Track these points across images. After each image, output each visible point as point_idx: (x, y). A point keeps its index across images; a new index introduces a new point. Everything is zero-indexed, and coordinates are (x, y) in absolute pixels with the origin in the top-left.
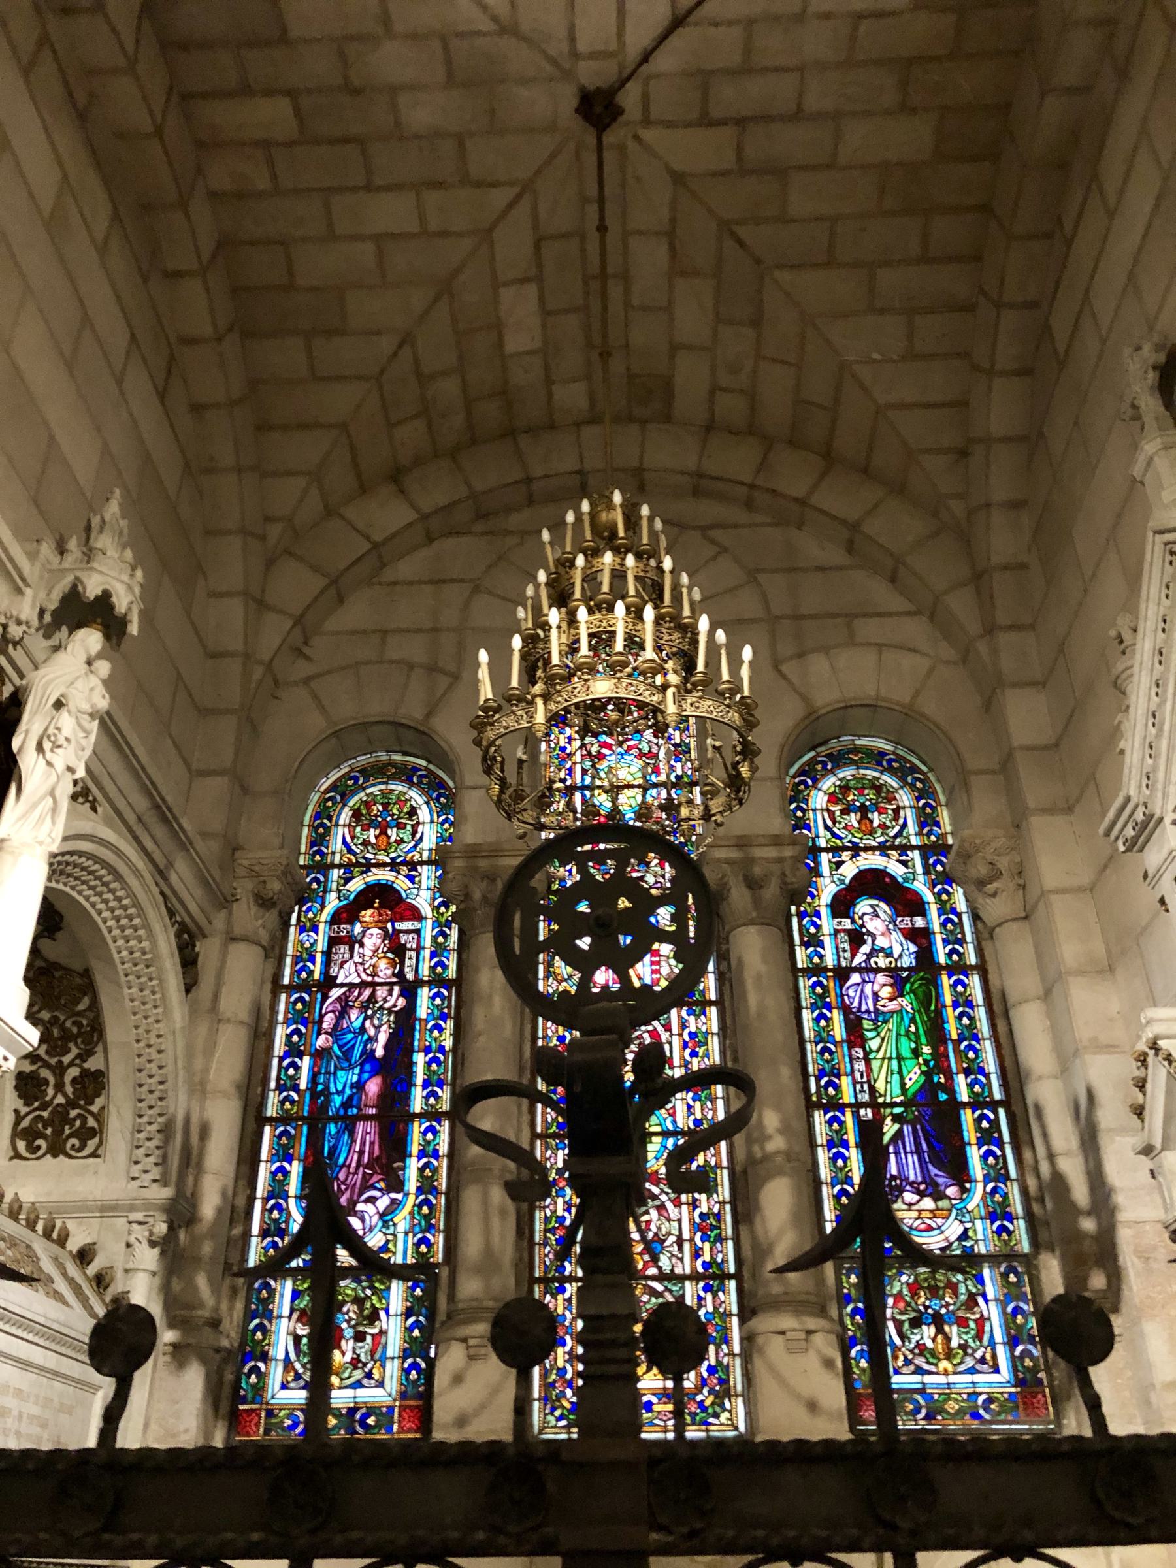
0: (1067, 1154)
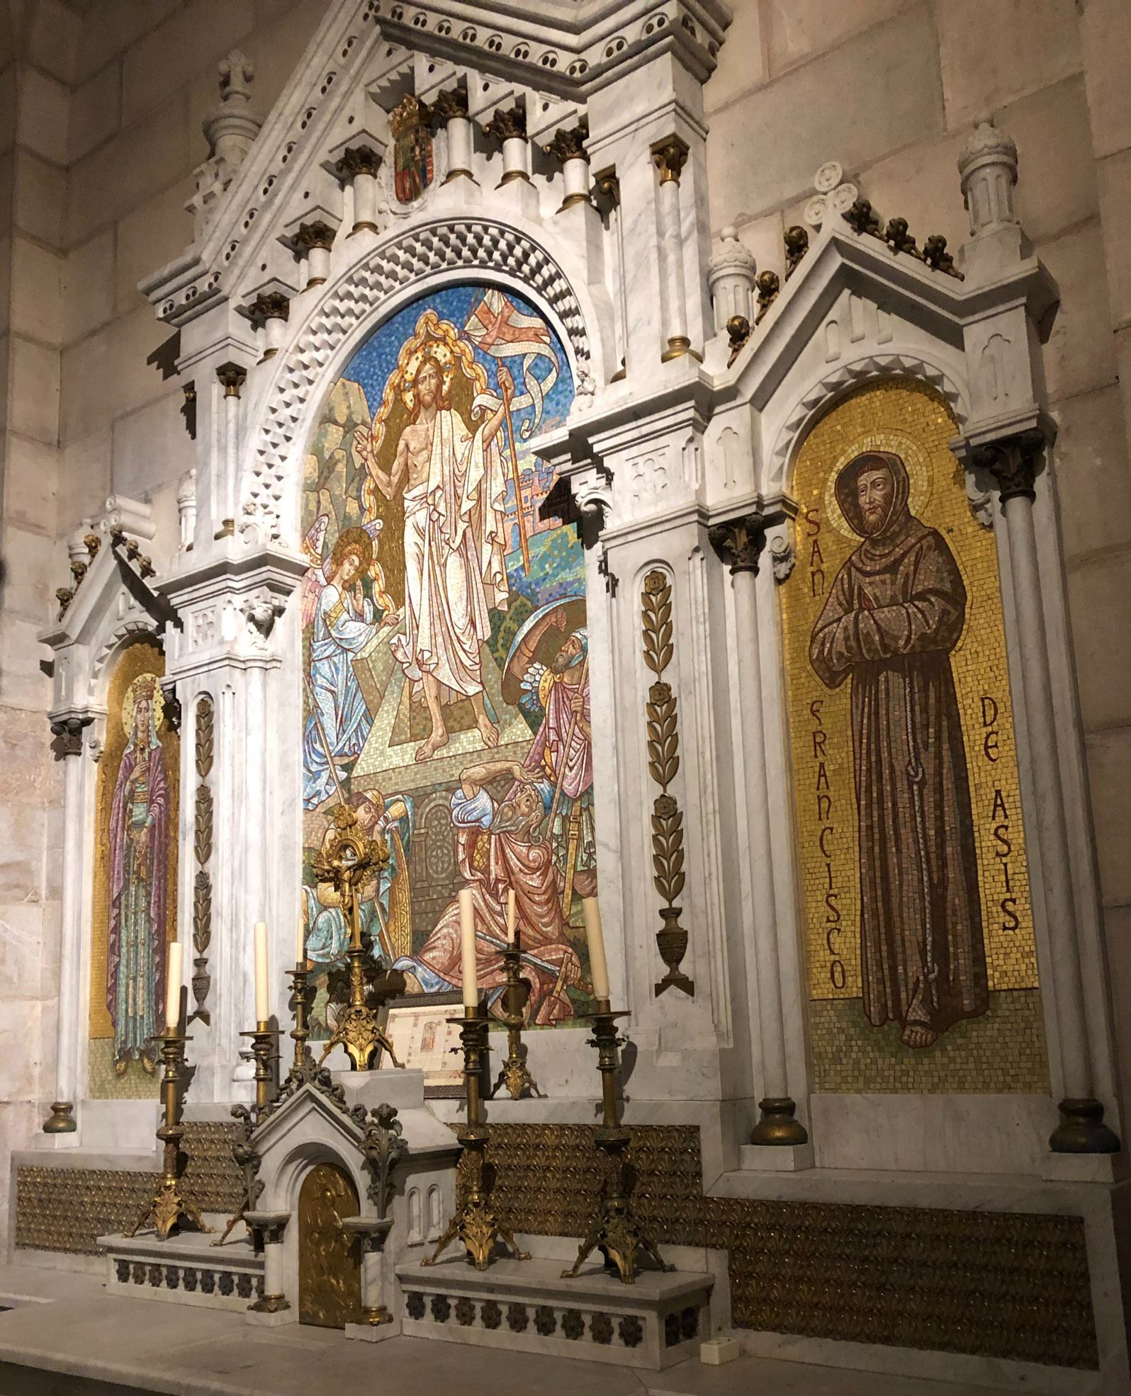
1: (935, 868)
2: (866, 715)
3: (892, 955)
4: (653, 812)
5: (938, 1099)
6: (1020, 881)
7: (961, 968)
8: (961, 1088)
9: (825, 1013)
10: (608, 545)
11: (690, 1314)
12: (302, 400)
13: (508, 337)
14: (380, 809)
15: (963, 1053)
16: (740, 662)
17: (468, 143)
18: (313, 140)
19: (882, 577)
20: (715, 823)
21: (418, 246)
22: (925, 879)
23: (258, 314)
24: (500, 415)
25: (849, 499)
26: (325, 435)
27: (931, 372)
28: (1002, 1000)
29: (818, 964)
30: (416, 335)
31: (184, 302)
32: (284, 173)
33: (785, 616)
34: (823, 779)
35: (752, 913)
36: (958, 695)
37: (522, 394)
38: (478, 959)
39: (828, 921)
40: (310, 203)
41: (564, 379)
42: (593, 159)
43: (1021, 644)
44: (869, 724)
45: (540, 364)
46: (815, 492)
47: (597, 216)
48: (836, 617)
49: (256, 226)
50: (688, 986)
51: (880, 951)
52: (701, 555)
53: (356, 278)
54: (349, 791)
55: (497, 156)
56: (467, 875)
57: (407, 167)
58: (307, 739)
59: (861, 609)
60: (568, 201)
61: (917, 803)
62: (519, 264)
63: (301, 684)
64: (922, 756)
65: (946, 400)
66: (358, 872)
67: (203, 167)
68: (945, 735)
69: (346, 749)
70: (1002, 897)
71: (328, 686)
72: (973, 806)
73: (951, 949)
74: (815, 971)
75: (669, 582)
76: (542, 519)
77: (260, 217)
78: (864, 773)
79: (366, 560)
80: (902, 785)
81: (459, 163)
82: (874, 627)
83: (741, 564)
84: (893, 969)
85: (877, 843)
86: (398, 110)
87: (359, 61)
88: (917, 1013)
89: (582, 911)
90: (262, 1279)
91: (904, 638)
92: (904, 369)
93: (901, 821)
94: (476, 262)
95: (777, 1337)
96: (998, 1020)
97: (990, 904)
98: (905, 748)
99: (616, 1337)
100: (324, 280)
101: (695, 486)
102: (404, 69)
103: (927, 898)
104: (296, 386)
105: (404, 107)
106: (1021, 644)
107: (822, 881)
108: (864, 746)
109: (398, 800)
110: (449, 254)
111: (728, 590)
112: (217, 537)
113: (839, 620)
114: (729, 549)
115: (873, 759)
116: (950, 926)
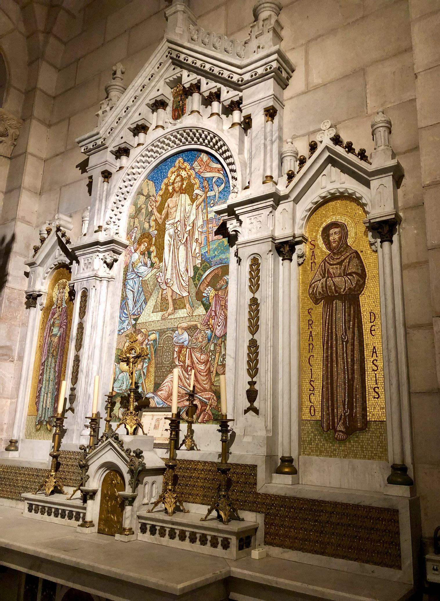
1: (350, 374)
2: (328, 315)
3: (333, 405)
5: (346, 461)
6: (381, 381)
7: (358, 411)
8: (355, 457)
9: (307, 425)
10: (239, 247)
12: (131, 186)
14: (146, 336)
15: (357, 444)
16: (283, 292)
17: (199, 102)
18: (144, 96)
19: (336, 266)
20: (270, 350)
21: (178, 135)
22: (346, 377)
24: (203, 197)
25: (326, 238)
26: (139, 199)
27: (358, 195)
28: (372, 425)
29: (305, 406)
30: (175, 167)
31: (92, 147)
32: (133, 106)
33: (300, 277)
34: (311, 338)
35: (282, 385)
36: (362, 311)
37: (212, 190)
39: (310, 390)
40: (140, 117)
41: (227, 187)
42: (243, 111)
43: (385, 295)
44: (329, 318)
45: (219, 181)
46: (314, 234)
47: (243, 131)
48: (319, 279)
53: (155, 144)
54: (135, 328)
55: (209, 107)
56: (177, 363)
57: (176, 108)
58: (122, 308)
59: (328, 277)
60: (233, 125)
61: (345, 349)
62: (214, 145)
63: (122, 288)
64: (347, 332)
65: (363, 205)
66: (136, 359)
67: (103, 101)
68: (356, 325)
69: (136, 313)
70: (374, 386)
71: (131, 289)
72: (365, 352)
73: (354, 404)
74: (304, 409)
75: (260, 261)
76: (215, 235)
77: (122, 121)
78: (326, 336)
79: (150, 244)
80: (340, 342)
81: (195, 108)
82: (332, 284)
84: (333, 410)
85: (329, 362)
86: (175, 88)
87: (163, 71)
88: (340, 427)
89: (219, 380)
90: (85, 514)
91: (343, 289)
92: (348, 194)
94: (199, 143)
96: (370, 432)
97: (369, 388)
98: (341, 328)
100: (143, 144)
101: (271, 228)
102: (179, 75)
103: (347, 384)
104: (130, 180)
105: (178, 88)
106: (385, 295)
107: (309, 375)
108: (327, 326)
109: (154, 333)
111: (281, 267)
112: (95, 232)
113: (320, 280)
114: (282, 252)
115: (330, 331)
116: (354, 395)
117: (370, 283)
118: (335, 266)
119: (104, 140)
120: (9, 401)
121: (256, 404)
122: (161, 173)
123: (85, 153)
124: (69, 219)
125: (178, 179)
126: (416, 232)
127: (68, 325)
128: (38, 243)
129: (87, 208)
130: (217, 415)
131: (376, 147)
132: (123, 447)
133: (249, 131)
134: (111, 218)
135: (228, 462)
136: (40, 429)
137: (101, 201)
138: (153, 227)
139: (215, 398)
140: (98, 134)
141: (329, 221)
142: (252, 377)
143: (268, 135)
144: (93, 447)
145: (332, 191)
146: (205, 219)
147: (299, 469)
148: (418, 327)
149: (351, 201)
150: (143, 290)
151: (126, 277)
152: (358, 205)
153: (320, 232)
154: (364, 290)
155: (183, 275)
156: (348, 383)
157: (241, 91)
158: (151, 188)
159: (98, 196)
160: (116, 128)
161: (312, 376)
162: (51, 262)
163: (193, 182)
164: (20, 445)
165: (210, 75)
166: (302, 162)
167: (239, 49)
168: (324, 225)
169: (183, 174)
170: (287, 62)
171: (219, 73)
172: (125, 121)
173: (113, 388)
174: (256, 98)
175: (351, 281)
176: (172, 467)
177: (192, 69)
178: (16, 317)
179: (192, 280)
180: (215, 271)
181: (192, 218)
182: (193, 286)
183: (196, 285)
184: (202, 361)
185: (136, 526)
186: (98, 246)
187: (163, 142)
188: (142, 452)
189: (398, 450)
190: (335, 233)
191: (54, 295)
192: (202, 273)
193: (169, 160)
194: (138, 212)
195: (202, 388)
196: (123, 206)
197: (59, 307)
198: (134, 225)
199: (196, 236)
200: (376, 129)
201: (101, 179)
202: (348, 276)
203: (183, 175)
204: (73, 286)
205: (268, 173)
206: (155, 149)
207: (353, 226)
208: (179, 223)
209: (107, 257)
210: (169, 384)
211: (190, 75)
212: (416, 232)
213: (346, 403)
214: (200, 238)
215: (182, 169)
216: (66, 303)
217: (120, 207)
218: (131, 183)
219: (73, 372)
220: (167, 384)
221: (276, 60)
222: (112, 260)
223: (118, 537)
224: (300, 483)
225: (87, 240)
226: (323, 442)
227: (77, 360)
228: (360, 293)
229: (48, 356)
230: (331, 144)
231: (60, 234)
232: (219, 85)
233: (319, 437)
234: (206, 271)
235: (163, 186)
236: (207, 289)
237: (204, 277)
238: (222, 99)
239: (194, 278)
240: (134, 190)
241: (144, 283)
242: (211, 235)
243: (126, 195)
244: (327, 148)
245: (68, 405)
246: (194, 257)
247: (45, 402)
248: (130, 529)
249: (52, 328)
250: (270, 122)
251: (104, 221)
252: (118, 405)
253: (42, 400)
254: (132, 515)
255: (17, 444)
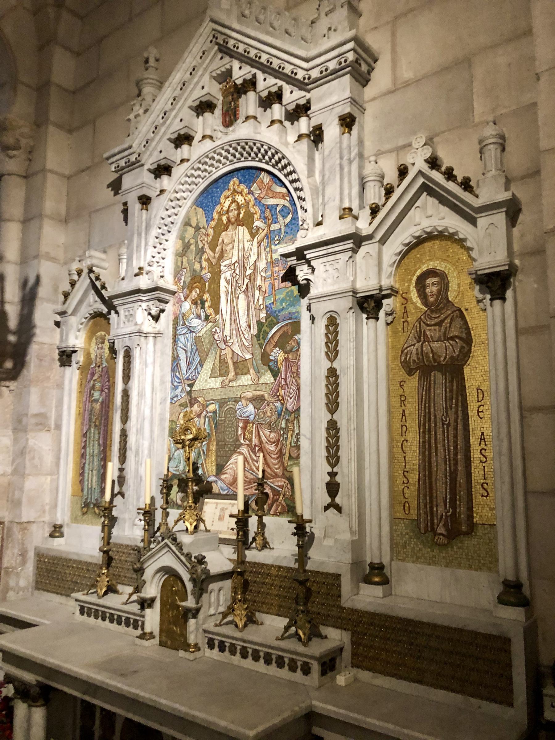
0: (11, 303)
1: (452, 465)
2: (424, 390)
4: (326, 426)
5: (448, 572)
8: (459, 566)
10: (311, 301)
11: (333, 660)
13: (271, 196)
14: (204, 407)
15: (461, 551)
16: (368, 360)
17: (256, 104)
18: (186, 95)
19: (435, 327)
20: (354, 434)
22: (448, 469)
23: (157, 172)
25: (422, 290)
28: (479, 528)
32: (172, 110)
33: (390, 340)
34: (404, 418)
36: (467, 386)
37: (276, 223)
38: (245, 480)
41: (295, 218)
44: (426, 394)
45: (284, 209)
46: (406, 284)
48: (413, 343)
49: (158, 133)
50: (339, 509)
51: (427, 508)
52: (353, 311)
53: (202, 161)
54: (191, 396)
55: (268, 110)
56: (242, 441)
57: (227, 111)
58: (173, 370)
59: (424, 341)
60: (300, 137)
61: (446, 434)
63: (171, 345)
64: (449, 412)
66: (193, 442)
68: (460, 404)
69: (190, 377)
70: (482, 481)
71: (183, 347)
72: (471, 438)
73: (458, 503)
75: (338, 321)
76: (282, 282)
77: (160, 130)
78: (422, 417)
80: (439, 424)
81: (251, 113)
82: (430, 350)
83: (371, 316)
84: (431, 508)
85: (427, 449)
86: (225, 84)
87: (208, 61)
88: (441, 530)
91: (444, 357)
93: (438, 441)
94: (257, 159)
95: (371, 674)
96: (477, 537)
97: (476, 484)
98: (442, 407)
99: (299, 670)
101: (352, 278)
102: (228, 66)
105: (227, 83)
108: (423, 404)
109: (213, 403)
110: (245, 154)
113: (414, 345)
114: (366, 308)
115: (427, 411)
116: (458, 492)
117: (477, 350)
118: (433, 328)
119: (139, 156)
120: (49, 478)
121: (338, 500)
122: (212, 197)
123: (116, 172)
124: (103, 256)
125: (234, 206)
126: (535, 286)
127: (111, 389)
128: (67, 287)
129: (123, 241)
130: (292, 507)
131: (485, 172)
132: (182, 550)
133: (320, 145)
134: (153, 257)
135: (307, 568)
136: (87, 512)
137: (139, 235)
138: (205, 268)
139: (289, 486)
140: (130, 147)
141: (424, 268)
142: (333, 466)
143: (345, 152)
144: (147, 549)
145: (428, 230)
146: (269, 261)
147: (391, 576)
148: (538, 409)
149: (452, 242)
150: (197, 349)
151: (176, 332)
152: (462, 248)
153: (414, 282)
154: (470, 360)
155: (244, 332)
156: (450, 476)
157: (308, 91)
158: (200, 217)
159: (136, 228)
160: (153, 139)
161: (405, 466)
162: (85, 311)
163: (252, 210)
164: (65, 530)
165: (267, 69)
166: (389, 191)
167: (304, 31)
168: (418, 273)
169: (240, 199)
170: (367, 50)
171: (280, 67)
172: (163, 129)
173: (168, 468)
174: (328, 102)
175: (453, 348)
176: (241, 574)
177: (245, 59)
178: (48, 378)
179: (255, 339)
180: (283, 328)
181: (253, 258)
182: (257, 346)
183: (261, 345)
184: (271, 440)
185: (203, 643)
186: (140, 294)
187: (213, 158)
188: (204, 557)
189: (510, 562)
190: (433, 284)
191: (92, 351)
192: (268, 330)
193: (221, 181)
194: (185, 249)
195: (273, 473)
196: (167, 241)
197: (99, 366)
198: (182, 265)
199: (259, 282)
200: (484, 146)
201: (138, 206)
202: (450, 341)
203: (239, 201)
204: (114, 343)
205: (346, 205)
206: (203, 167)
207: (455, 275)
208: (236, 264)
209: (152, 307)
210: (234, 466)
211: (243, 68)
212: (535, 286)
213: (448, 501)
214: (263, 285)
215: (238, 193)
216: (107, 362)
217: (164, 242)
218: (175, 211)
219: (120, 449)
220: (231, 466)
221: (354, 50)
222: (158, 312)
223: (181, 653)
224: (393, 593)
225: (126, 287)
226: (420, 546)
227: (124, 434)
228: (465, 364)
229: (90, 426)
230: (425, 168)
231: (93, 276)
232: (280, 83)
233: (415, 540)
234: (272, 328)
235: (215, 216)
236: (274, 351)
237: (270, 335)
238: (284, 102)
239: (258, 336)
240: (180, 220)
241: (198, 340)
242: (277, 281)
243: (170, 227)
244: (420, 172)
245: (117, 489)
246: (258, 309)
247: (90, 481)
248: (196, 645)
249: (92, 391)
250: (347, 135)
251: (145, 261)
252: (175, 489)
253: (86, 478)
254: (197, 629)
255: (62, 529)
